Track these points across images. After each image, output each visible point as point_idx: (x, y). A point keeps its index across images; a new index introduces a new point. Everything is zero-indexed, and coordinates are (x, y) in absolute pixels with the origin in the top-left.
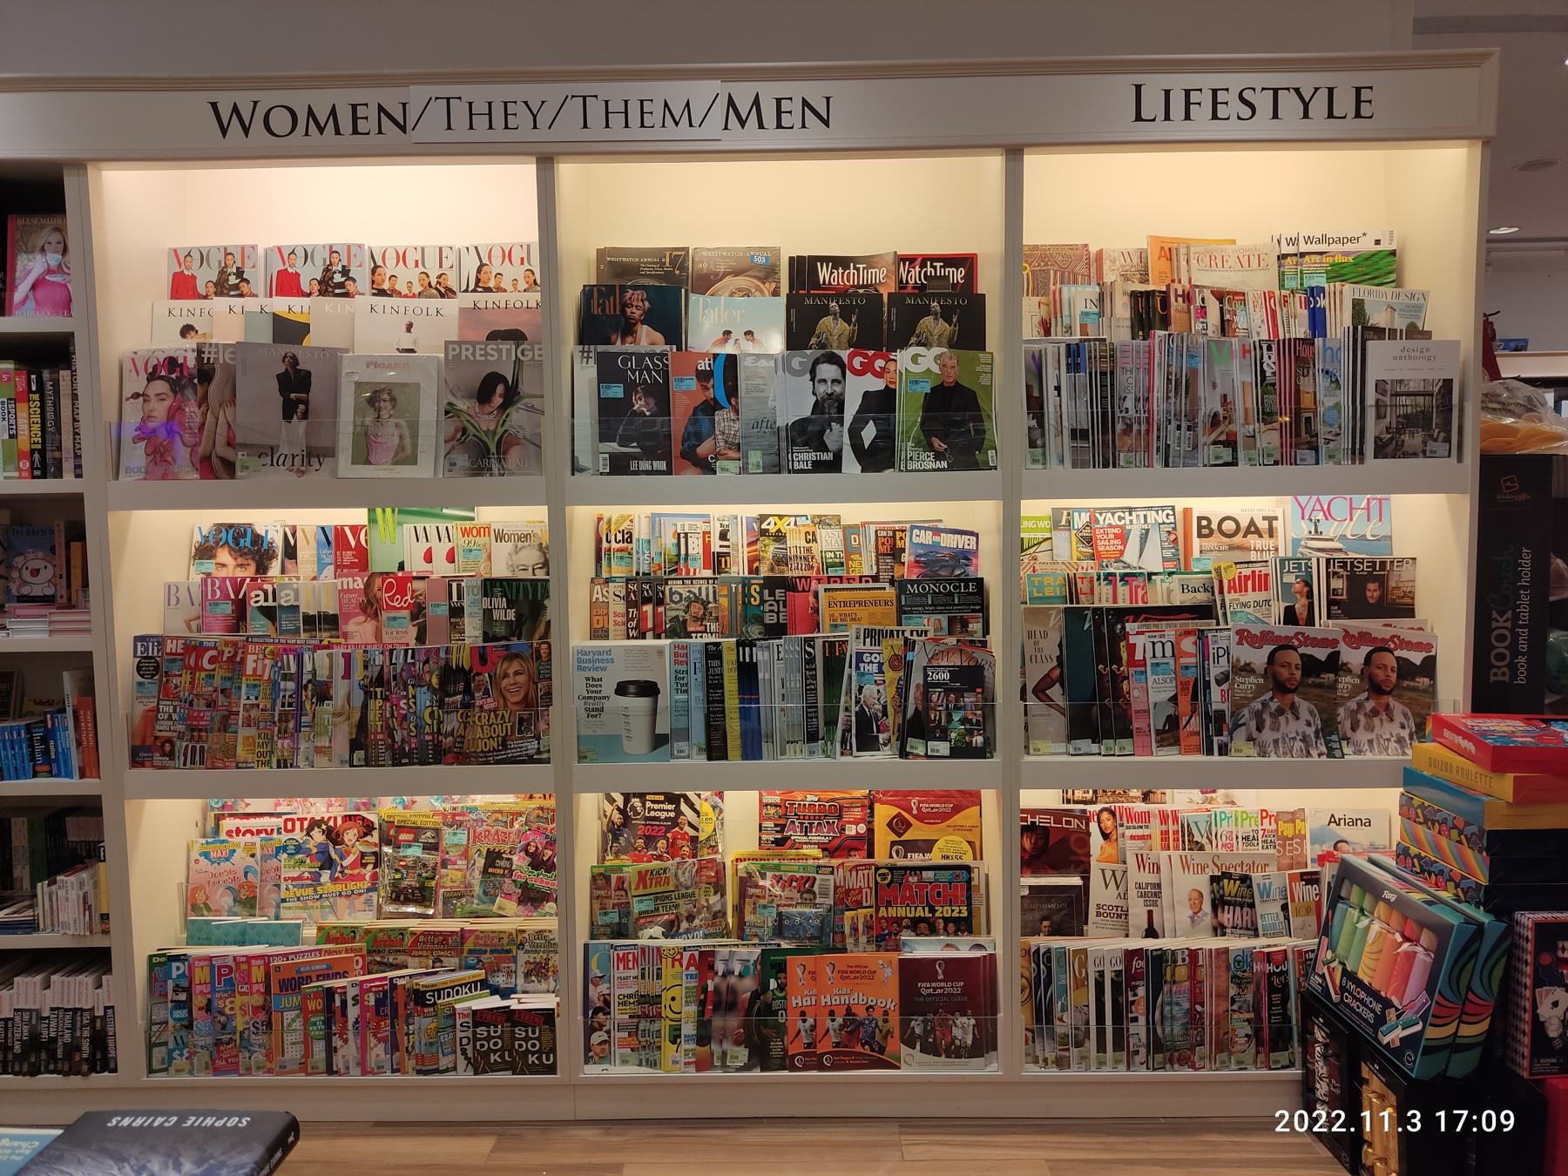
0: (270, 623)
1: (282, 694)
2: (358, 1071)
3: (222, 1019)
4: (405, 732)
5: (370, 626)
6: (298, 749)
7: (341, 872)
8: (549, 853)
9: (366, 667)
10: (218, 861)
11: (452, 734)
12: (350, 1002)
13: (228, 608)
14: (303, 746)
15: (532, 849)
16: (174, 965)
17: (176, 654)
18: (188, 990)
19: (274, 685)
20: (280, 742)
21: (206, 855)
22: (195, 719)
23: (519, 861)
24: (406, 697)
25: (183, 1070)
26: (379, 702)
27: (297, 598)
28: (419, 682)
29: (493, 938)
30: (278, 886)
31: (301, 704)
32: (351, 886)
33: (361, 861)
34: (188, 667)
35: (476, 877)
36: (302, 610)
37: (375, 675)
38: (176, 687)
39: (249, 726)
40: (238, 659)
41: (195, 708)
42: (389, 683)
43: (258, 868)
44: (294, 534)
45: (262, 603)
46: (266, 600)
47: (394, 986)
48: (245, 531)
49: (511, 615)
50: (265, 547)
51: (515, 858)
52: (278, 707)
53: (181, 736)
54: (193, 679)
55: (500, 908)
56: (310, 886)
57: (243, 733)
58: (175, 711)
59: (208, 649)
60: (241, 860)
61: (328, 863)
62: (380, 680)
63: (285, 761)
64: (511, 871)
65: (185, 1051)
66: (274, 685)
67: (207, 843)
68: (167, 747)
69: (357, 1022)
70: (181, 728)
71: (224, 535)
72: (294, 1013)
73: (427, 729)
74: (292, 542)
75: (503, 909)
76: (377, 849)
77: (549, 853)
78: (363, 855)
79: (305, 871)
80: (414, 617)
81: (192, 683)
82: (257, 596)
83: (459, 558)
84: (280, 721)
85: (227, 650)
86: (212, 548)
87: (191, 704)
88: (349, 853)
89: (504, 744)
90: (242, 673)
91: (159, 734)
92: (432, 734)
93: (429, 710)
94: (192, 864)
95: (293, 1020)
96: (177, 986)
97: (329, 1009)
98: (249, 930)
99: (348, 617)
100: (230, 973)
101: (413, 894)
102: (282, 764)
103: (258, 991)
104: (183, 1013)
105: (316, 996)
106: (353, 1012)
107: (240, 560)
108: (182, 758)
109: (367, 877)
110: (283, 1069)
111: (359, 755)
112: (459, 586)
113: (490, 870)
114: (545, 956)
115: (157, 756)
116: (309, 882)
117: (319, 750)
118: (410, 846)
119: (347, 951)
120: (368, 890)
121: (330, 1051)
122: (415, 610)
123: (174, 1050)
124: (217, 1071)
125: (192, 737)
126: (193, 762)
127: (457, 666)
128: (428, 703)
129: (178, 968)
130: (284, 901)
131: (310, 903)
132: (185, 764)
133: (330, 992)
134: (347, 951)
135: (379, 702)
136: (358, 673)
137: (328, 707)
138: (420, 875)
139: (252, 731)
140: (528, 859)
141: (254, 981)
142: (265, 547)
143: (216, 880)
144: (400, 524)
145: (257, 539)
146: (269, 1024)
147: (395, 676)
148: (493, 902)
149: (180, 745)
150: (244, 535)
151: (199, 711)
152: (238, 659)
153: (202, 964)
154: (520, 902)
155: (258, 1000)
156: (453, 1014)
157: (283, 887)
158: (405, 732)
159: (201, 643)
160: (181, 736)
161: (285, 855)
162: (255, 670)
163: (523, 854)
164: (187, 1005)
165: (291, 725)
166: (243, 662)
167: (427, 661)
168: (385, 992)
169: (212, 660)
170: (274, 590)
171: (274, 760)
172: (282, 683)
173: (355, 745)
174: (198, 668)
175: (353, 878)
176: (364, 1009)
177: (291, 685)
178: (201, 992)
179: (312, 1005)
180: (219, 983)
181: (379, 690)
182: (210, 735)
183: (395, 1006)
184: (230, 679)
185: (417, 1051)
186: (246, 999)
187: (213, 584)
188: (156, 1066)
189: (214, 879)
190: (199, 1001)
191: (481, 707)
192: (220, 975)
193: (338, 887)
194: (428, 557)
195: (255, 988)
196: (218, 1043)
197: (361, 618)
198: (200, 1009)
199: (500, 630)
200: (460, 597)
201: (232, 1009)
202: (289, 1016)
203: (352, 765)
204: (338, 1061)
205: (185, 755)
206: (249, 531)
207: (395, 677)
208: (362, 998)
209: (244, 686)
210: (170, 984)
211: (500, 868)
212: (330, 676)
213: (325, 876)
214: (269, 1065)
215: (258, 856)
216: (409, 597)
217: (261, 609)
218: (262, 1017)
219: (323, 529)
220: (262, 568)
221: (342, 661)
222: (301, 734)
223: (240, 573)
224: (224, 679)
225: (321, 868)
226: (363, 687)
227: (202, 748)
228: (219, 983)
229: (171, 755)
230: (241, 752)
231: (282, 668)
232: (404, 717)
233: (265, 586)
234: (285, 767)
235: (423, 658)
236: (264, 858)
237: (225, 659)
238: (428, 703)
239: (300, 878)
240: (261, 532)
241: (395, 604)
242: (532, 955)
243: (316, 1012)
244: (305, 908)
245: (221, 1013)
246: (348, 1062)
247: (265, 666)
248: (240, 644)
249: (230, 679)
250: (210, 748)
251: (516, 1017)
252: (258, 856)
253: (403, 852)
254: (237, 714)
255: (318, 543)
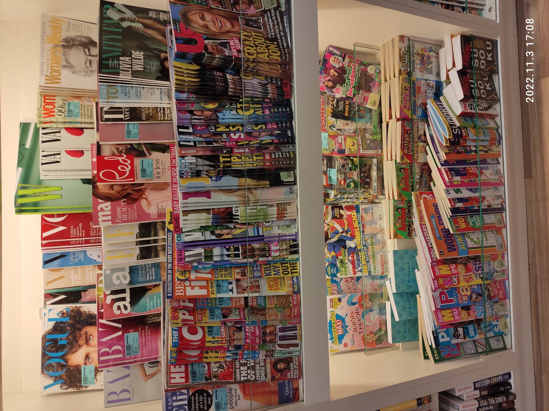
0: (149, 293)
1: (226, 258)
2: (501, 188)
3: (474, 296)
4: (262, 134)
5: (151, 195)
6: (280, 236)
7: (347, 232)
8: (332, 71)
9: (198, 174)
10: (345, 327)
11: (264, 86)
12: (460, 195)
13: (133, 337)
14: (276, 231)
15: (330, 84)
16: (441, 340)
17: (186, 372)
18: (456, 326)
19: (217, 267)
20: (273, 254)
21: (341, 338)
22: (253, 341)
23: (340, 93)
24: (228, 134)
25: (505, 323)
26: (234, 159)
27: (123, 269)
28: (213, 121)
29: (406, 95)
30: (358, 278)
31: (235, 240)
32: (356, 225)
33: (338, 218)
34: (200, 357)
35: (351, 127)
36: (134, 261)
37: (207, 163)
38: (221, 367)
39: (258, 287)
40: (191, 305)
41: (242, 343)
42: (214, 149)
43: (349, 295)
44: (54, 295)
45: (127, 303)
46: (124, 299)
47: (445, 163)
48: (50, 340)
49: (136, 54)
50: (67, 319)
51: (338, 96)
52: (240, 260)
53: (270, 353)
54: (212, 349)
55: (374, 104)
56: (357, 255)
57: (265, 291)
58: (245, 365)
59: (181, 337)
60: (343, 309)
61: (341, 242)
62: (213, 159)
63: (292, 246)
64: (348, 98)
65: (494, 323)
66: (217, 267)
67: (332, 339)
68: (281, 366)
69: (471, 190)
70: (262, 355)
71: (53, 362)
72: (468, 240)
73: (260, 113)
74: (63, 297)
75: (375, 102)
76: (330, 207)
77: (332, 71)
78: (334, 217)
79: (347, 258)
80: (142, 154)
81: (216, 349)
82: (119, 308)
83: (79, 121)
84: (253, 256)
85: (181, 317)
86: (69, 371)
87: (238, 347)
88: (333, 228)
89: (274, 40)
90: (206, 299)
91: (269, 377)
92: (263, 109)
93: (240, 111)
94: (348, 348)
95: (472, 240)
96: (454, 336)
97: (465, 211)
98: (401, 290)
99: (142, 213)
100: (444, 293)
101: (365, 172)
102: (294, 249)
103: (456, 269)
104: (471, 328)
105: (456, 222)
106: (465, 193)
107: (82, 342)
108: (291, 349)
109: (349, 213)
110: (503, 246)
111: (284, 176)
112: (107, 113)
113: (346, 115)
114: (416, 56)
115: (290, 375)
116: (355, 256)
117: (281, 215)
118: (330, 178)
119: (418, 205)
120: (358, 211)
121: (490, 210)
122: (134, 153)
123: (494, 332)
124: (506, 297)
125: (272, 341)
126: (294, 337)
127: (144, 329)
128: (234, 112)
129: (443, 337)
130: (370, 273)
131: (370, 253)
132: (296, 345)
133: (454, 210)
134: (418, 205)
135: (234, 159)
136: (205, 182)
137: (240, 212)
138: (350, 169)
139: (263, 283)
140: (338, 86)
141: (449, 272)
142: (67, 319)
143: (358, 327)
144: (40, 182)
145: (58, 328)
146: (476, 259)
147: (208, 143)
148: (370, 110)
149: (279, 353)
150: (55, 341)
151: (246, 338)
152: (191, 305)
153: (440, 317)
154: (369, 90)
155: (461, 269)
156: (463, 115)
157: (359, 274)
158: (262, 134)
159: (174, 345)
160: (270, 353)
161: (338, 275)
162: (201, 287)
163: (334, 90)
164: (464, 325)
165: (256, 246)
166: (192, 300)
167: (191, 112)
168: (450, 170)
169: (193, 331)
170: (114, 292)
171: (291, 257)
172: (215, 259)
173: (277, 182)
174: (202, 346)
175: (350, 224)
176: (463, 184)
177: (217, 251)
178: (459, 315)
179: (463, 226)
180: (452, 301)
181: (222, 160)
182: (269, 323)
183: (459, 162)
184: (212, 311)
185: (487, 144)
186: (461, 278)
187: (106, 354)
188: (501, 345)
189: (358, 329)
190: (464, 317)
191: (239, 51)
192: (447, 301)
193: (357, 233)
194: (79, 153)
195: (454, 271)
196: (490, 297)
197: (143, 203)
198: (469, 315)
199: (155, 66)
200: (118, 110)
201: (467, 290)
202: (470, 244)
203: (294, 183)
204: (495, 204)
205: (288, 346)
206: (49, 337)
207: (208, 143)
208: (458, 185)
209: (219, 296)
210: (454, 341)
211: (344, 108)
212: (207, 211)
213: (350, 244)
214: (500, 258)
215: (339, 296)
216: (120, 159)
217: (132, 303)
218: (471, 265)
219: (46, 263)
220: (90, 320)
221: (191, 200)
222: (266, 234)
223: (94, 341)
224: (212, 316)
225: (345, 247)
226: (219, 176)
227: (282, 330)
228: (452, 301)
229: (288, 361)
230: (284, 291)
231: (199, 262)
232: (249, 134)
233: (108, 301)
234: (296, 246)
235: (188, 116)
236: (340, 292)
237: (192, 318)
238: (234, 112)
239: (353, 263)
240: (52, 324)
241: (128, 170)
242: (416, 66)
243: (467, 223)
244: (374, 256)
245: (471, 297)
246: (495, 196)
247: (197, 279)
248: (175, 304)
249: (212, 311)
250: (281, 322)
251: (467, 65)
252: (339, 296)
253: (334, 182)
254: (246, 299)
255: (63, 265)
